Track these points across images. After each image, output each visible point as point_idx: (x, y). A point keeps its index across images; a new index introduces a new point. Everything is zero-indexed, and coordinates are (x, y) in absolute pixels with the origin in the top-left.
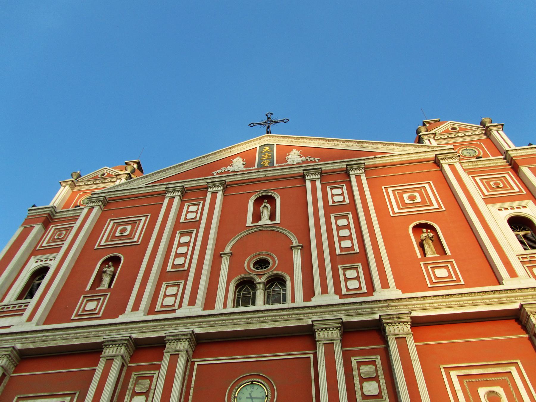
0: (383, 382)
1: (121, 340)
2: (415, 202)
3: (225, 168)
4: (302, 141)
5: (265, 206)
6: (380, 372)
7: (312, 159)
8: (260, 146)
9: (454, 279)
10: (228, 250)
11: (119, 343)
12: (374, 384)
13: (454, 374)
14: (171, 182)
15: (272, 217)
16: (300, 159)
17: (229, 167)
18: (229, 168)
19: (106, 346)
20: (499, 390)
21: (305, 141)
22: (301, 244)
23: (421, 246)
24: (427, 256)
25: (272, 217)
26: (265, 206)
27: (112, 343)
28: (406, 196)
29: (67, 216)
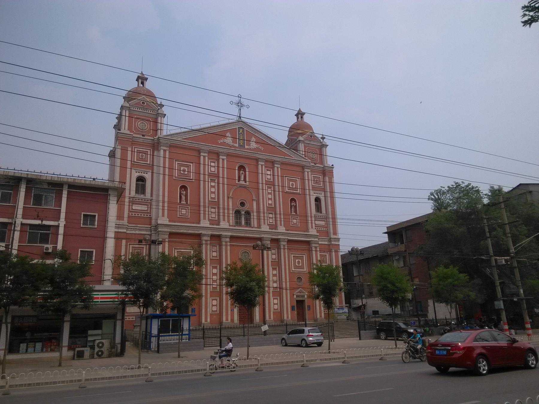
0: (277, 255)
1: (208, 235)
2: (293, 187)
3: (223, 139)
4: (257, 132)
5: (243, 173)
6: (276, 253)
7: (260, 147)
8: (238, 128)
9: (298, 224)
10: (231, 195)
11: (207, 235)
12: (275, 255)
13: (292, 255)
14: (201, 143)
15: (245, 180)
16: (255, 145)
17: (225, 139)
18: (225, 141)
19: (203, 236)
20: (300, 260)
21: (258, 133)
22: (256, 199)
23: (291, 206)
24: (292, 213)
25: (245, 180)
26: (243, 173)
27: (205, 235)
28: (291, 183)
29: (140, 141)
